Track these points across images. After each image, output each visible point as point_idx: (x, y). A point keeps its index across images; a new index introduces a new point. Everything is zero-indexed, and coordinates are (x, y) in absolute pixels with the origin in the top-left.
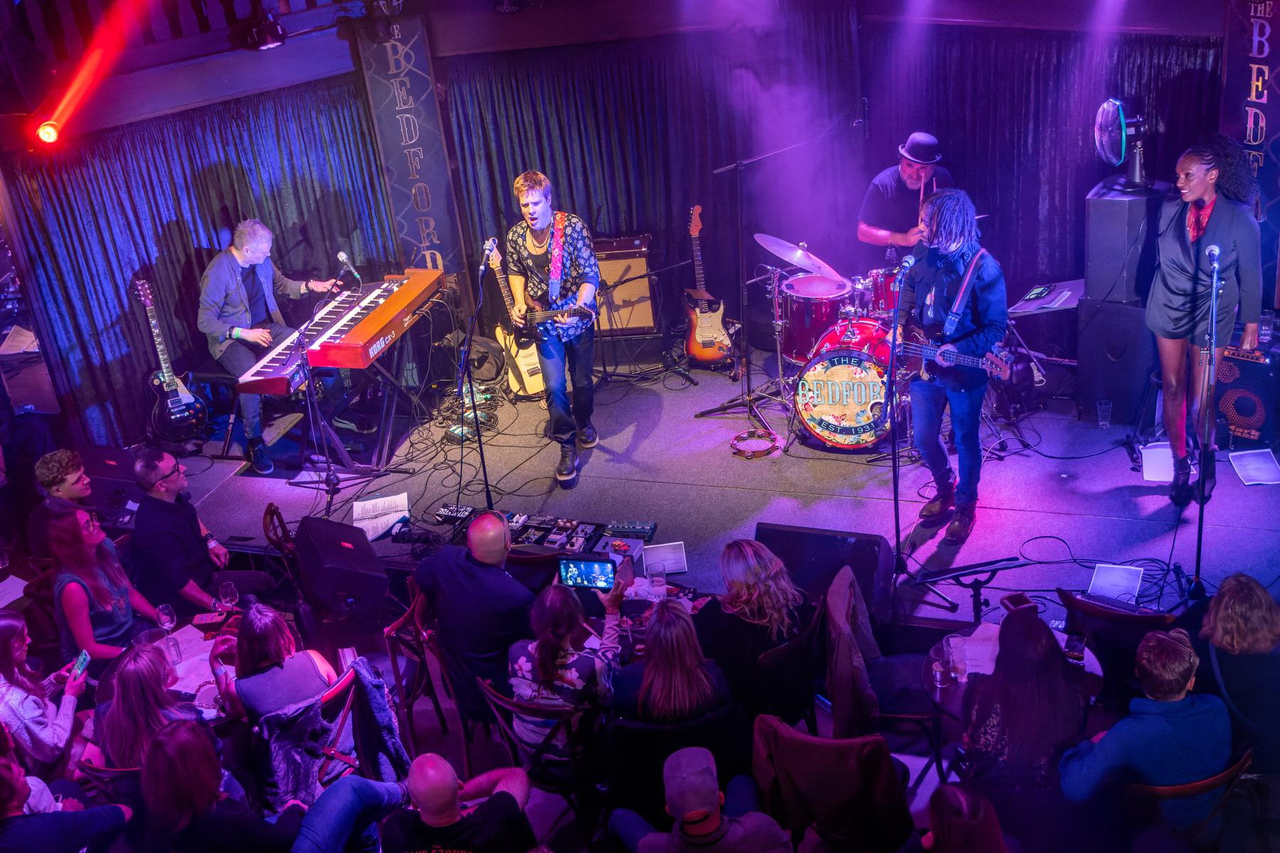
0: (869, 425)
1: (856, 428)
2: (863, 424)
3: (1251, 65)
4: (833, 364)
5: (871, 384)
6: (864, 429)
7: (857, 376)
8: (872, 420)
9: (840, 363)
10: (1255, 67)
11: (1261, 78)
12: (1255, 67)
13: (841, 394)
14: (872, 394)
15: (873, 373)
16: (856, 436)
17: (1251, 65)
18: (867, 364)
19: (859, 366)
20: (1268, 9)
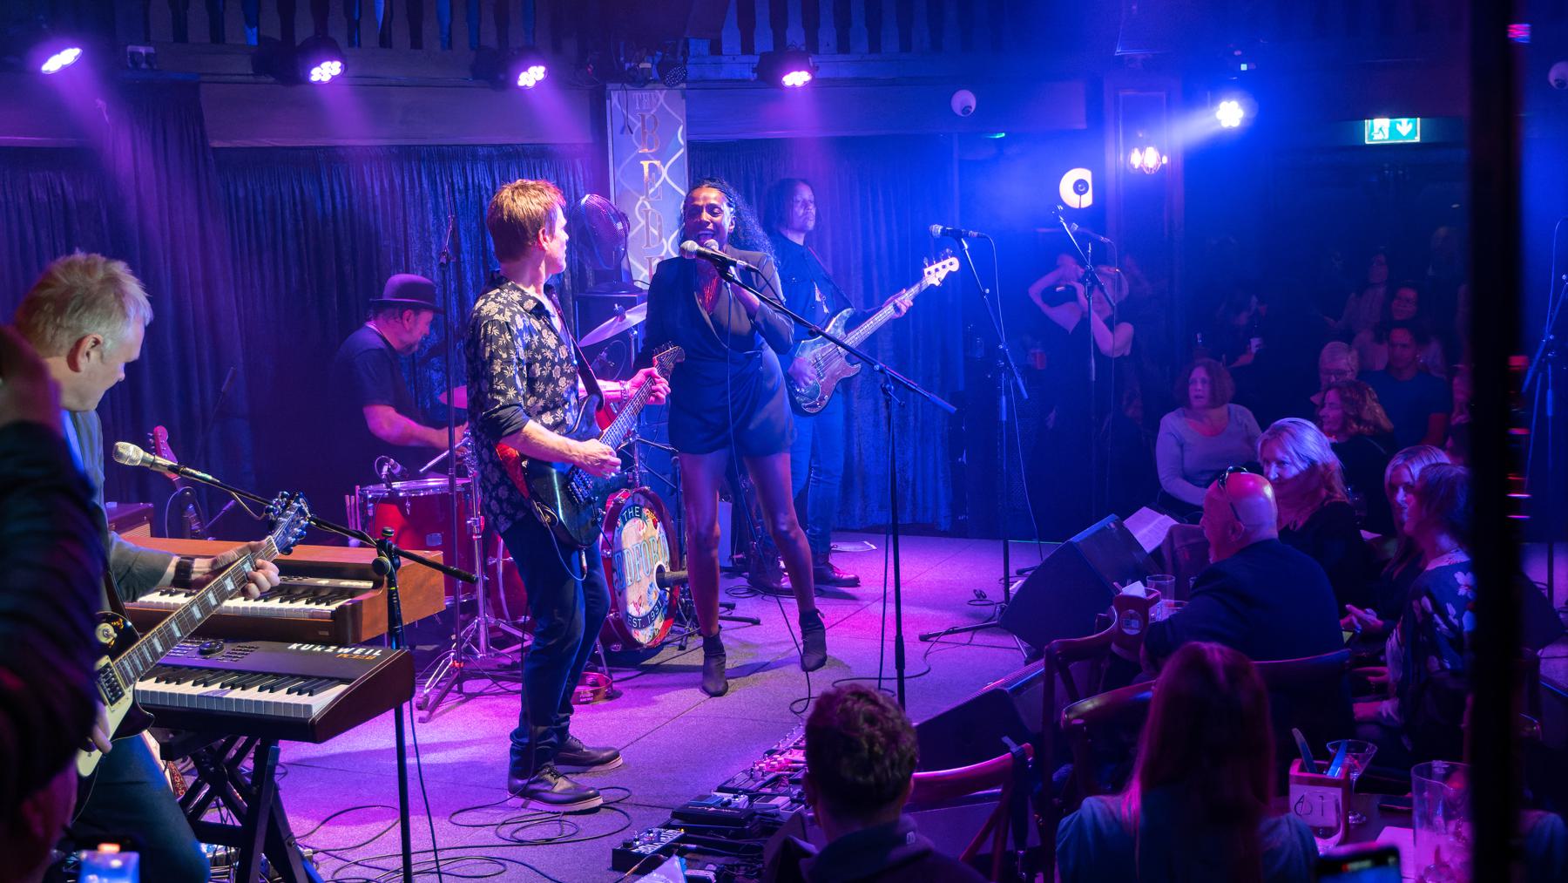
0: (657, 604)
1: (649, 614)
2: (654, 604)
3: (642, 162)
4: (625, 523)
5: (651, 540)
6: (655, 612)
7: (641, 533)
8: (658, 595)
9: (628, 519)
10: (645, 164)
11: (653, 174)
12: (645, 164)
13: (635, 565)
14: (654, 555)
15: (650, 523)
16: (650, 627)
17: (642, 162)
18: (646, 512)
19: (640, 517)
20: (654, 100)
